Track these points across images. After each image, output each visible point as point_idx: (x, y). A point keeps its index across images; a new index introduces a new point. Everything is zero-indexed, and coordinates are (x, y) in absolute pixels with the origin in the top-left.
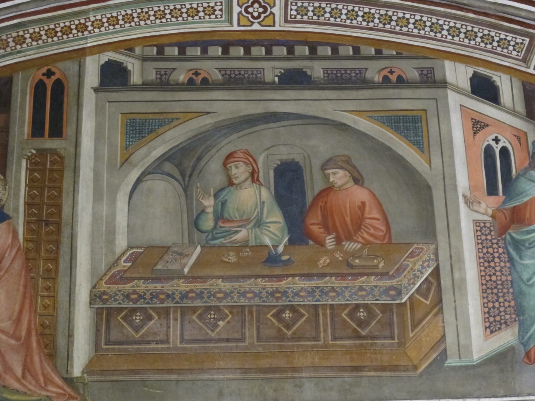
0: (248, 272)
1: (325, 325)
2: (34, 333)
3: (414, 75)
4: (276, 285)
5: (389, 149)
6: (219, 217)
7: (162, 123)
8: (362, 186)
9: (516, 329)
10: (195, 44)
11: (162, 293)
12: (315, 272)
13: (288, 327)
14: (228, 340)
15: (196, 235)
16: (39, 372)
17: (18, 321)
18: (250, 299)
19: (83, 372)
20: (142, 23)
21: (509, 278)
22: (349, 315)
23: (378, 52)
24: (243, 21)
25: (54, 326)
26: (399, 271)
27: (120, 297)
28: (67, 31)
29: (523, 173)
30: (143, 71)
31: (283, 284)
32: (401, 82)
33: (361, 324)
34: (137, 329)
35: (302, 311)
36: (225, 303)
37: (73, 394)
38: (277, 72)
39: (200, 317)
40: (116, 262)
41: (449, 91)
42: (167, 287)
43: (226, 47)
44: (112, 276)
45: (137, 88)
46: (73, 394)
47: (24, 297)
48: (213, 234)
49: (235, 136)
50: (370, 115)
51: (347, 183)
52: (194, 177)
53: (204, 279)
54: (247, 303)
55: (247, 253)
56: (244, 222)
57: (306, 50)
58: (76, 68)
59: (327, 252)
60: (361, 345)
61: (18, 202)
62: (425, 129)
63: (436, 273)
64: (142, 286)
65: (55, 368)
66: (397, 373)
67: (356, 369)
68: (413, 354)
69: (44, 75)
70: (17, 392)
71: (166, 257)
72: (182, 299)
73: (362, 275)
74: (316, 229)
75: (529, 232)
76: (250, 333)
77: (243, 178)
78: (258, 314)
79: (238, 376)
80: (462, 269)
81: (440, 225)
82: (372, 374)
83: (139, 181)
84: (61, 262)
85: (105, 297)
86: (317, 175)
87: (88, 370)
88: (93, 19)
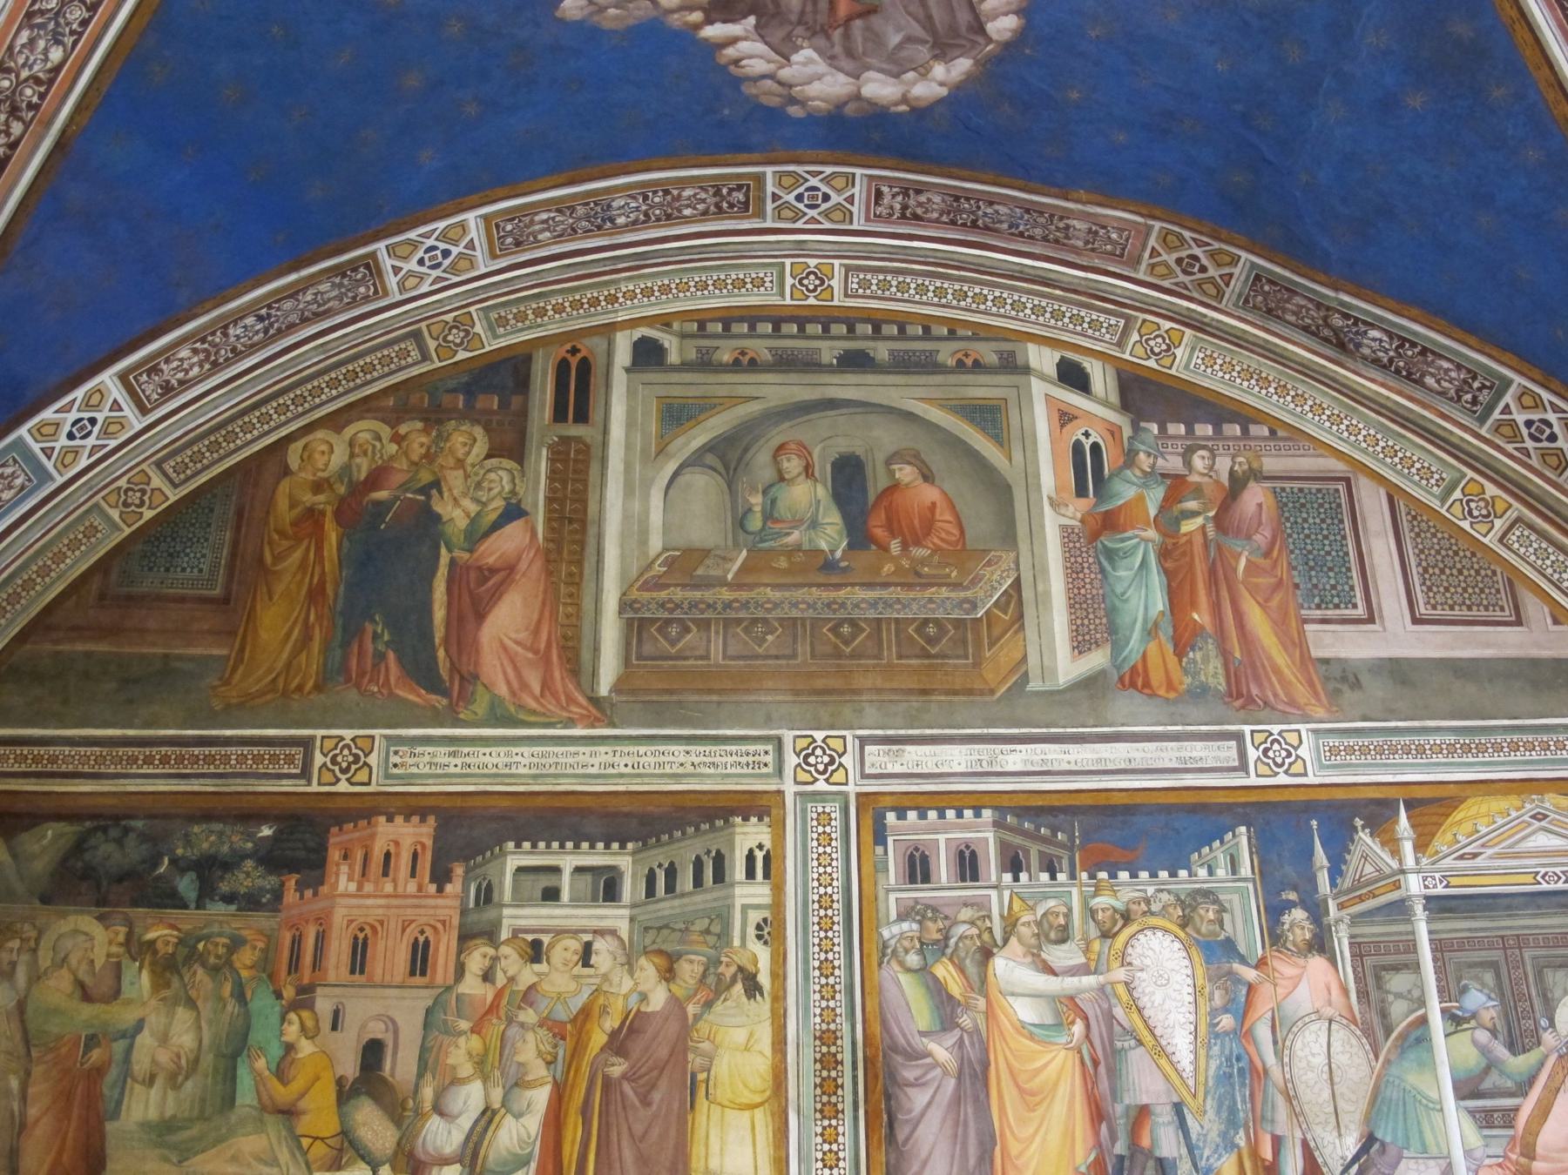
0: (800, 580)
1: (889, 641)
2: (554, 645)
3: (993, 359)
4: (833, 594)
6: (769, 515)
7: (703, 409)
8: (933, 483)
9: (1109, 651)
10: (741, 320)
11: (702, 601)
12: (878, 580)
13: (847, 643)
14: (777, 657)
15: (742, 536)
16: (560, 688)
17: (536, 631)
18: (802, 611)
19: (610, 691)
20: (681, 295)
21: (1101, 592)
22: (917, 630)
23: (952, 332)
24: (797, 295)
26: (974, 583)
28: (594, 302)
29: (1116, 473)
30: (681, 350)
31: (842, 594)
32: (978, 367)
33: (931, 641)
34: (673, 643)
35: (863, 625)
36: (774, 614)
37: (599, 715)
38: (836, 353)
39: (747, 630)
40: (650, 566)
41: (1032, 378)
42: (708, 595)
43: (777, 323)
44: (646, 582)
46: (599, 715)
47: (544, 603)
48: (762, 535)
49: (787, 424)
50: (944, 404)
51: (916, 479)
53: (751, 587)
54: (799, 615)
56: (797, 523)
57: (869, 329)
58: (605, 346)
59: (893, 559)
60: (930, 665)
62: (1004, 419)
63: (1017, 584)
64: (678, 594)
65: (578, 685)
66: (971, 698)
67: (924, 692)
68: (989, 676)
69: (568, 352)
70: (534, 712)
71: (708, 562)
72: (724, 609)
73: (932, 585)
74: (879, 533)
75: (1123, 540)
76: (803, 649)
77: (796, 471)
78: (812, 626)
79: (790, 698)
80: (1047, 580)
82: (943, 698)
84: (586, 565)
85: (636, 606)
86: (881, 469)
87: (617, 688)
88: (624, 289)
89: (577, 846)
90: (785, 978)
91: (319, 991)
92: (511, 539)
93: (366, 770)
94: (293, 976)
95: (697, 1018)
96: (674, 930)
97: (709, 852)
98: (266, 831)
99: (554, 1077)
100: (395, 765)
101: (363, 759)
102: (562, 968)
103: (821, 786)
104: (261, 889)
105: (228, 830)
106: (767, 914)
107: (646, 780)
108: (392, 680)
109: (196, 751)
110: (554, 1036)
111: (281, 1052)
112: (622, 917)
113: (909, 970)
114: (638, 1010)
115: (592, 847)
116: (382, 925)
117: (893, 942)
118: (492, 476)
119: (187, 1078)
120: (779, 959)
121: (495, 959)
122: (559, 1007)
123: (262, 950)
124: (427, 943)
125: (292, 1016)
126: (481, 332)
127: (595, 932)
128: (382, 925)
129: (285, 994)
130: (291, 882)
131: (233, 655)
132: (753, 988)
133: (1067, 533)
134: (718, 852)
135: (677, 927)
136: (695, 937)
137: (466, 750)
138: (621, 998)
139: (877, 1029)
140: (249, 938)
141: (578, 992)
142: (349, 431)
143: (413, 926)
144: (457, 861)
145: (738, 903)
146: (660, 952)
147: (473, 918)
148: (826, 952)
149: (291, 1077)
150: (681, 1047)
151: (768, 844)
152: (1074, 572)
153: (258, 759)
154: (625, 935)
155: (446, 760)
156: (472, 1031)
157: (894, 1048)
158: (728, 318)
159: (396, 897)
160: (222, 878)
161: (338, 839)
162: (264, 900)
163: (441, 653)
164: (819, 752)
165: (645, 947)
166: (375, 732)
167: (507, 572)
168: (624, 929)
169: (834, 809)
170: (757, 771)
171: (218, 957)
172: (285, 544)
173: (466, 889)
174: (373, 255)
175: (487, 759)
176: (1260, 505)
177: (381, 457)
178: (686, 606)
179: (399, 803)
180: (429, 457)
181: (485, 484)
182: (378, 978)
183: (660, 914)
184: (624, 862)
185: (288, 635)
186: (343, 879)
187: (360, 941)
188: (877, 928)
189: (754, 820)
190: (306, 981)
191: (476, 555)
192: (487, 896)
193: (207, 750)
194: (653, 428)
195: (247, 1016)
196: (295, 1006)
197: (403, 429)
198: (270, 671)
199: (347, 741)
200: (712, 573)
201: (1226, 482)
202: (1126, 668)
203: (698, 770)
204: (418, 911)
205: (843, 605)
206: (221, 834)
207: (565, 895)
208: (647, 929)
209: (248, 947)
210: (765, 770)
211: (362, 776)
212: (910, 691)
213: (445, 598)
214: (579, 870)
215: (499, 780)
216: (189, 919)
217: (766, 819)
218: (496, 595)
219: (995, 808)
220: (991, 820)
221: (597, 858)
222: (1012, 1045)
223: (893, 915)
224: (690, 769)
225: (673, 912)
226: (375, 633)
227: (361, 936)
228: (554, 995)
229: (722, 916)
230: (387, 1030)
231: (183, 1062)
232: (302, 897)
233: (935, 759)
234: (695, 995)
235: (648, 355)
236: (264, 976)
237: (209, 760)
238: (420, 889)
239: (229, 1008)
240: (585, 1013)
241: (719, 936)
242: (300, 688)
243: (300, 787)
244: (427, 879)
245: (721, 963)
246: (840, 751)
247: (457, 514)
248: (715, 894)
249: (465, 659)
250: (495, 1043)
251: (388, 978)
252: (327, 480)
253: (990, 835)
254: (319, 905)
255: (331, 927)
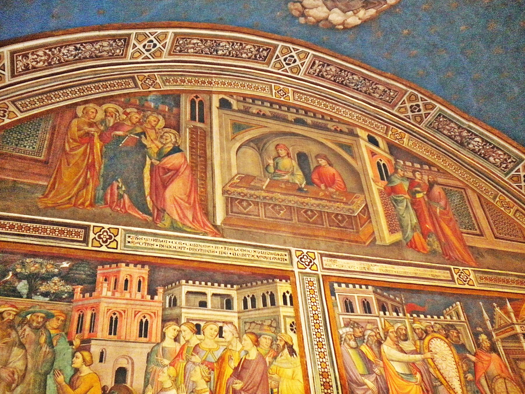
2: (197, 202)
4: (303, 200)
5: (341, 155)
6: (276, 167)
7: (248, 127)
11: (254, 194)
14: (285, 219)
15: (267, 174)
16: (201, 220)
17: (189, 196)
19: (221, 224)
22: (335, 217)
23: (331, 119)
25: (206, 200)
26: (353, 203)
27: (235, 193)
28: (204, 82)
31: (306, 200)
32: (341, 132)
37: (217, 232)
38: (293, 117)
39: (272, 208)
40: (233, 178)
42: (257, 193)
44: (231, 184)
45: (234, 111)
47: (191, 185)
49: (278, 138)
52: (263, 151)
53: (273, 192)
54: (291, 205)
55: (289, 185)
59: (322, 191)
60: (341, 230)
61: (186, 145)
63: (366, 206)
64: (245, 191)
65: (208, 220)
67: (341, 240)
71: (254, 181)
73: (338, 202)
74: (316, 181)
75: (399, 197)
77: (284, 155)
78: (297, 211)
79: (292, 235)
81: (365, 187)
82: (347, 243)
83: (240, 147)
84: (208, 174)
87: (224, 222)
89: (213, 285)
90: (304, 348)
91: (93, 342)
92: (175, 160)
93: (115, 243)
94: (79, 334)
95: (271, 363)
96: (257, 324)
97: (268, 292)
98: (65, 265)
99: (210, 389)
100: (129, 242)
101: (113, 238)
102: (211, 337)
103: (308, 270)
104: (63, 292)
105: (45, 262)
106: (293, 320)
107: (239, 260)
108: (127, 206)
109: (29, 225)
110: (209, 369)
111: (72, 373)
112: (234, 316)
113: (352, 348)
114: (245, 358)
115: (219, 285)
116: (125, 312)
117: (344, 336)
118: (166, 134)
119: (17, 386)
120: (301, 340)
121: (180, 331)
122: (210, 356)
123: (62, 321)
124: (147, 322)
125: (78, 354)
126: (159, 82)
127: (224, 322)
128: (125, 312)
129: (74, 343)
130: (79, 289)
131: (49, 186)
132: (292, 352)
133: (380, 192)
134: (271, 292)
135: (258, 323)
136: (266, 328)
137: (161, 239)
138: (237, 353)
139: (344, 372)
140: (55, 314)
141: (217, 349)
142: (105, 107)
143: (139, 314)
144: (160, 286)
145: (282, 314)
146: (253, 333)
147: (168, 312)
148: (319, 338)
149: (77, 385)
150: (265, 376)
151: (290, 292)
152: (385, 205)
153: (62, 232)
154: (236, 323)
155: (152, 242)
156: (170, 365)
157: (352, 381)
158: (254, 99)
159: (131, 300)
160: (41, 285)
161: (101, 271)
162: (64, 297)
163: (148, 199)
164: (305, 257)
165: (245, 331)
166: (120, 227)
167: (176, 171)
168: (236, 321)
169: (314, 279)
170: (282, 262)
171: (38, 323)
172: (75, 144)
173: (164, 299)
174: (129, 35)
175: (171, 244)
176: (439, 192)
177: (119, 119)
178: (248, 195)
179: (131, 258)
180: (140, 123)
181: (164, 137)
182: (123, 338)
183: (250, 317)
184: (233, 293)
185: (79, 179)
186: (105, 290)
187: (114, 319)
188: (337, 329)
189: (284, 281)
190: (86, 336)
191: (161, 163)
192: (174, 303)
193: (35, 225)
194: (230, 130)
195: (54, 353)
196: (79, 349)
197: (128, 110)
198: (69, 194)
199: (106, 229)
200: (257, 185)
201: (428, 184)
202: (408, 240)
203: (260, 259)
204: (142, 307)
205: (307, 204)
206: (41, 264)
207: (209, 305)
208: (245, 323)
209: (55, 318)
210: (285, 262)
211: (114, 245)
212: (335, 239)
213: (149, 177)
214: (214, 295)
215: (176, 253)
216: (22, 303)
217: (289, 281)
218: (171, 180)
219: (373, 286)
220: (372, 290)
221: (222, 290)
222: (397, 382)
223: (343, 325)
224: (257, 258)
225: (256, 316)
226: (118, 186)
227: (114, 317)
228: (207, 350)
229: (275, 321)
230: (128, 364)
231: (16, 377)
232: (84, 297)
233: (349, 265)
234: (269, 353)
235: (224, 104)
236: (63, 333)
237: (36, 229)
238: (143, 297)
239: (44, 349)
240: (222, 359)
241: (276, 328)
242: (83, 204)
243: (83, 246)
244: (146, 293)
245: (277, 339)
246: (314, 258)
247: (153, 146)
248: (272, 310)
249: (159, 203)
250: (182, 371)
251: (128, 338)
252: (95, 123)
253: (373, 296)
254: (92, 301)
255: (98, 312)
